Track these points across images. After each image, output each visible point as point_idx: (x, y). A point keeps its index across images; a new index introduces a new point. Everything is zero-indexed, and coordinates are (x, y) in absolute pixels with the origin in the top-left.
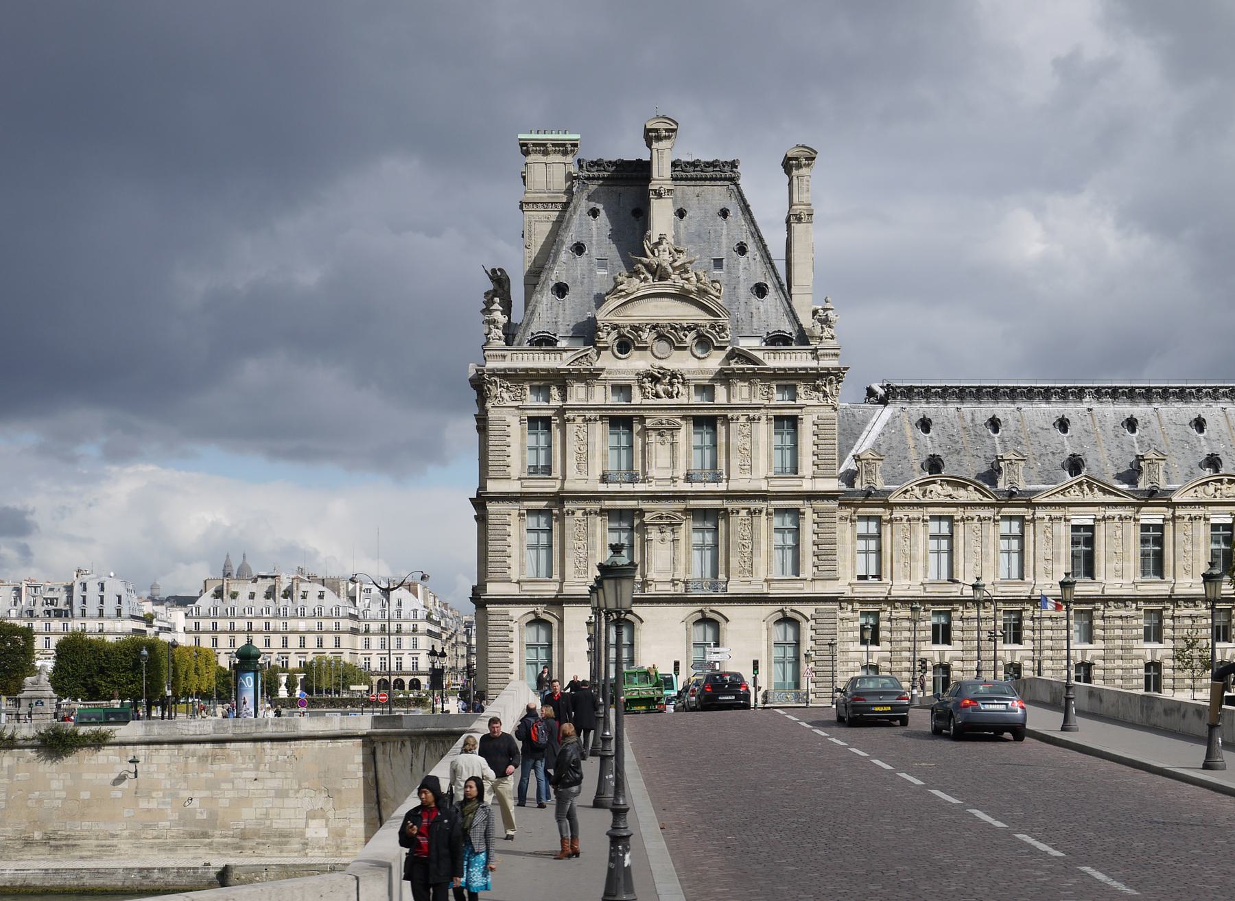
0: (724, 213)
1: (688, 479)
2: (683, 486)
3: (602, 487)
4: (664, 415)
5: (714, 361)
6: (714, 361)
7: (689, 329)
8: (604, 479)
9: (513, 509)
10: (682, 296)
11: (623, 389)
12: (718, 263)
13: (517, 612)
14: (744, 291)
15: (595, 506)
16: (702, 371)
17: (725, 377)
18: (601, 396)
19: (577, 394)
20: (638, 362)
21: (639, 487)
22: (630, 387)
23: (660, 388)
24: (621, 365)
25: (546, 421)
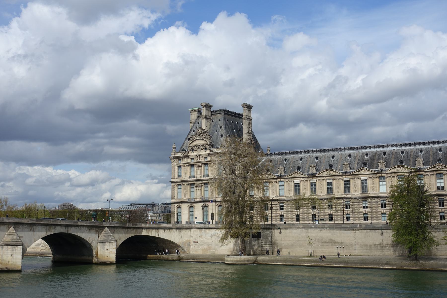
0: (220, 120)
1: (204, 177)
2: (202, 178)
3: (189, 179)
4: (198, 164)
5: (208, 151)
6: (208, 151)
7: (202, 146)
8: (190, 177)
9: (176, 184)
10: (202, 139)
11: (192, 159)
12: (216, 131)
13: (176, 205)
14: (219, 136)
15: (187, 183)
16: (206, 154)
17: (209, 155)
18: (189, 160)
19: (185, 160)
20: (196, 153)
21: (195, 179)
22: (193, 159)
23: (198, 158)
24: (193, 154)
25: (181, 166)
